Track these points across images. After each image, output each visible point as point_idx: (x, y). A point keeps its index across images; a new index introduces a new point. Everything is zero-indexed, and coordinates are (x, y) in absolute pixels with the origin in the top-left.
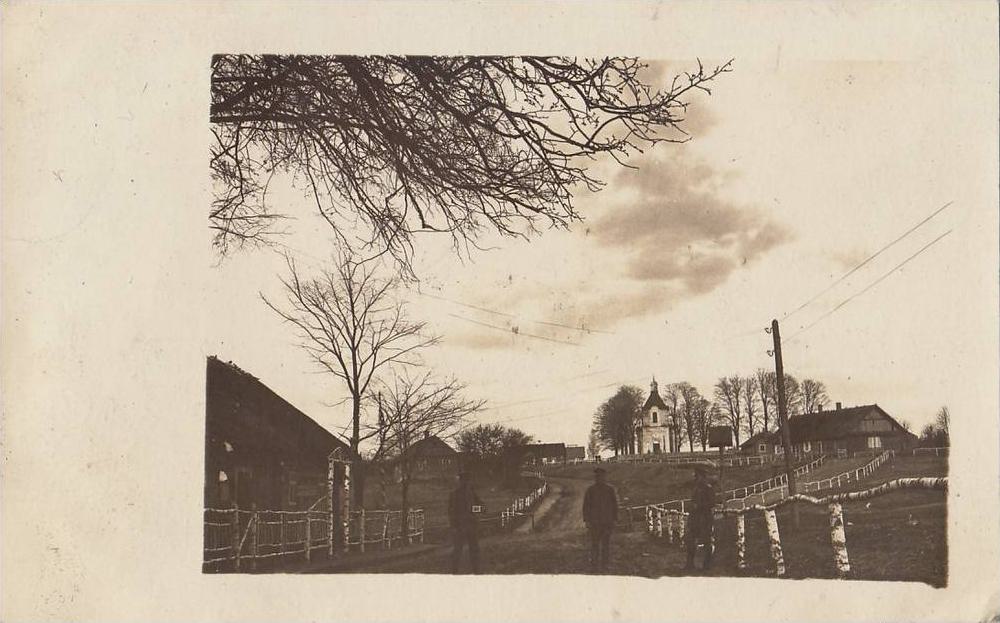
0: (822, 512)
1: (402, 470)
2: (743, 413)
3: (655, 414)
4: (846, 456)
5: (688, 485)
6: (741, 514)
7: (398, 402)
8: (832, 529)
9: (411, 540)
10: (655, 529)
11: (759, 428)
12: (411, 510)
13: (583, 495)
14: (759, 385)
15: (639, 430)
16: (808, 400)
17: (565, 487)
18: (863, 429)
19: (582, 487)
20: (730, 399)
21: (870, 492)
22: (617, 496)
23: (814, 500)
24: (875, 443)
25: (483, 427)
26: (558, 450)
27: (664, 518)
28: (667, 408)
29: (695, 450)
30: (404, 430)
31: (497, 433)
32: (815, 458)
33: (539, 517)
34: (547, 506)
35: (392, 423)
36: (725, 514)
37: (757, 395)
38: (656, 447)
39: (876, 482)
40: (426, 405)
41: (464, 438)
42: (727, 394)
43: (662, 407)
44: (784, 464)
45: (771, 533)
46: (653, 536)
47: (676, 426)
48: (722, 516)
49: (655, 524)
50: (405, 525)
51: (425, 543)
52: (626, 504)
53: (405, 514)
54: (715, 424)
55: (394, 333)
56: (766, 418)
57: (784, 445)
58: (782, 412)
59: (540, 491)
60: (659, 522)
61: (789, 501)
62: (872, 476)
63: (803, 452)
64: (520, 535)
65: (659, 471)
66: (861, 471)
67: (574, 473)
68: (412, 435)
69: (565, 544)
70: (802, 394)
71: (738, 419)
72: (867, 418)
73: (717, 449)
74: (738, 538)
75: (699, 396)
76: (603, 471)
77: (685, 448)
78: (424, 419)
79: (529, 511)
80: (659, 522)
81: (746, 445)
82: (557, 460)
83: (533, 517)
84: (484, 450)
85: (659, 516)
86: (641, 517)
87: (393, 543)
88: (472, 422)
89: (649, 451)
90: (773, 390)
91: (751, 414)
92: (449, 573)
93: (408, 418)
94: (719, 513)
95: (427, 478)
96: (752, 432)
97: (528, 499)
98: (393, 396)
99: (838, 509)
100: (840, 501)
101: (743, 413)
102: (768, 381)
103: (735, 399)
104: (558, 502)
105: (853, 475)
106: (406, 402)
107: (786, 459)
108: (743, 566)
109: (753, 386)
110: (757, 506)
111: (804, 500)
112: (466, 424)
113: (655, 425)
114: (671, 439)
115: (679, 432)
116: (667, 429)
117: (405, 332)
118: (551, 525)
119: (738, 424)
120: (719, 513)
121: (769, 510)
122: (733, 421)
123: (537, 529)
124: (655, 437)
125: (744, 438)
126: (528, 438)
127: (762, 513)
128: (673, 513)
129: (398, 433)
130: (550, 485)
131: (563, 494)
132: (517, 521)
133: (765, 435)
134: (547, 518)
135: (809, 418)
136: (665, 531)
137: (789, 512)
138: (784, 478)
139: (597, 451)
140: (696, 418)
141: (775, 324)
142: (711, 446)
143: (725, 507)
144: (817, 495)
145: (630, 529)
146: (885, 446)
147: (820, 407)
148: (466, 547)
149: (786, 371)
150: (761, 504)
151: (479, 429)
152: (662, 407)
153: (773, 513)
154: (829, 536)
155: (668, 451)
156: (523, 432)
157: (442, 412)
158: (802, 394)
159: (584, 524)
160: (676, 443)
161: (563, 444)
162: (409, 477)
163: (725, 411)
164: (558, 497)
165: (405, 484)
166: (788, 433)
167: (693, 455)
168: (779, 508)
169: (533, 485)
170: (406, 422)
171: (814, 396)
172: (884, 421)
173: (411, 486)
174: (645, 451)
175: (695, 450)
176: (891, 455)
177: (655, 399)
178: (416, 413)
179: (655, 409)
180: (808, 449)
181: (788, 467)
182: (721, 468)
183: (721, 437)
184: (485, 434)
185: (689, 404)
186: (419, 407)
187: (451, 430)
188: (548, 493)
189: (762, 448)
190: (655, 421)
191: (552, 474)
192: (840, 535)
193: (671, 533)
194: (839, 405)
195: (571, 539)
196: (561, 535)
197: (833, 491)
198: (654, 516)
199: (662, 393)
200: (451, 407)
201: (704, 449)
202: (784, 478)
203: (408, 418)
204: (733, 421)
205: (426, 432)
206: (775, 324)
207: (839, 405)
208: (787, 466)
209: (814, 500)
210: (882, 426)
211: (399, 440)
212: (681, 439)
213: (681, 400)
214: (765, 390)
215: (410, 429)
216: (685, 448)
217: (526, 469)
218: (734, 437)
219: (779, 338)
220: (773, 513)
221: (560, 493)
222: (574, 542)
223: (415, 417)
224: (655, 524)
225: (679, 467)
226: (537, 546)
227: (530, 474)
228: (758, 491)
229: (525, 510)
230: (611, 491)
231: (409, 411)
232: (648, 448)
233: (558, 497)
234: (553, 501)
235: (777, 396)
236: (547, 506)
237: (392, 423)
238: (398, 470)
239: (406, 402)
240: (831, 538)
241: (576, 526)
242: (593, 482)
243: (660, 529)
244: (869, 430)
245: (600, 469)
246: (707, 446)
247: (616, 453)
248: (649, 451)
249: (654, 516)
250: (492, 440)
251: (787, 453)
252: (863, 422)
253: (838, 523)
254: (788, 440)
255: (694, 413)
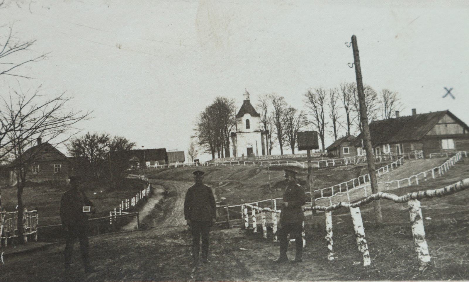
0: (403, 208)
1: (17, 174)
2: (328, 120)
3: (248, 121)
4: (422, 156)
5: (280, 184)
6: (328, 210)
7: (12, 112)
8: (412, 223)
9: (26, 238)
10: (251, 225)
11: (342, 133)
12: (26, 211)
13: (184, 194)
14: (341, 94)
15: (234, 135)
16: (386, 106)
17: (167, 188)
18: (438, 133)
19: (184, 187)
20: (315, 107)
21: (446, 190)
22: (215, 196)
23: (395, 197)
24: (448, 144)
25: (92, 134)
26: (160, 154)
27: (258, 215)
28: (258, 115)
29: (285, 153)
30: (18, 138)
31: (103, 140)
32: (394, 158)
33: (144, 216)
34: (150, 206)
35: (7, 131)
36: (314, 211)
37: (340, 103)
38: (250, 150)
39: (452, 180)
40: (38, 114)
41: (75, 145)
42: (312, 102)
43: (255, 114)
44: (366, 164)
45: (356, 228)
46: (249, 232)
47: (267, 132)
48: (310, 213)
49: (251, 220)
50: (20, 223)
51: (39, 240)
52: (223, 203)
53: (20, 214)
54: (303, 129)
55: (7, 48)
56: (349, 124)
57: (366, 148)
58: (363, 118)
59: (144, 192)
60: (254, 219)
61: (372, 199)
62: (446, 175)
63: (382, 153)
64: (131, 232)
65: (253, 173)
66: (436, 170)
67: (178, 175)
68: (26, 142)
69: (169, 241)
70: (380, 102)
71: (323, 125)
72: (440, 122)
73: (305, 152)
74: (326, 233)
75: (286, 104)
76: (201, 173)
77: (276, 151)
78: (36, 128)
79: (136, 210)
80: (254, 219)
81: (331, 149)
82: (160, 164)
83: (138, 215)
84: (92, 155)
85: (254, 213)
86: (236, 214)
87: (9, 241)
88: (79, 131)
89: (243, 155)
90: (354, 97)
91: (334, 121)
92: (152, 150)
93: (22, 126)
94: (308, 210)
95: (40, 181)
96: (336, 136)
97: (133, 200)
98: (7, 107)
99: (416, 205)
100: (419, 198)
101: (328, 120)
102: (350, 90)
103: (320, 107)
104: (161, 202)
105: (429, 175)
106: (20, 112)
107: (368, 160)
108: (332, 258)
109: (336, 95)
110: (343, 204)
111: (385, 198)
112: (75, 131)
113: (248, 130)
114: (263, 144)
115: (270, 137)
116: (259, 134)
117: (17, 48)
118: (155, 224)
119: (323, 128)
120: (308, 210)
121: (354, 207)
122: (319, 127)
123: (143, 227)
124: (247, 140)
125: (329, 141)
126: (132, 144)
127: (347, 210)
128: (266, 211)
129: (13, 140)
130: (153, 186)
131: (165, 195)
132: (124, 221)
133: (348, 140)
134: (151, 216)
135: (389, 122)
136: (260, 227)
137: (373, 208)
138: (366, 177)
139: (196, 155)
140: (285, 124)
141: (354, 40)
142: (300, 149)
143: (314, 205)
144: (399, 192)
145: (227, 226)
146: (459, 147)
147: (397, 112)
148: (77, 245)
149: (365, 82)
150: (346, 201)
151: (88, 137)
152: (255, 114)
153: (358, 209)
154: (409, 229)
155: (260, 154)
156: (127, 139)
157: (50, 121)
158: (380, 102)
159: (185, 222)
160: (267, 148)
161: (165, 149)
162: (23, 180)
163: (311, 118)
164: (161, 197)
165: (20, 187)
166: (369, 137)
167: (284, 158)
168: (364, 204)
169: (139, 186)
170: (20, 130)
171: (392, 103)
172: (456, 125)
173: (25, 189)
174: (239, 155)
175: (285, 153)
176: (463, 155)
177: (247, 108)
178: (30, 121)
179: (247, 116)
180: (387, 150)
181: (370, 169)
182: (310, 169)
183: (308, 141)
184: (93, 141)
185: (278, 113)
186: (32, 116)
187: (62, 137)
188: (152, 194)
189: (346, 151)
190: (248, 127)
191: (157, 177)
192: (419, 229)
193: (265, 228)
194: (414, 110)
195: (173, 236)
196: (164, 232)
197: (412, 189)
198: (250, 214)
199: (254, 103)
200: (62, 116)
201: (293, 153)
202: (366, 177)
203: (22, 126)
204: (319, 127)
205: (39, 139)
206: (354, 40)
207: (414, 110)
208: (369, 166)
209: (395, 197)
210: (453, 129)
211: (14, 147)
212: (272, 143)
213: (271, 109)
214: (346, 97)
215: (24, 136)
216: (276, 151)
217: (130, 172)
218: (320, 141)
219: (358, 51)
220: (358, 209)
221: (163, 194)
222: (176, 238)
223: (28, 125)
224: (251, 220)
225: (271, 168)
226: (142, 242)
227: (135, 176)
228: (344, 190)
229: (131, 209)
230: (209, 190)
231: (22, 120)
232: (242, 151)
233: (161, 197)
234: (157, 201)
235: (358, 104)
236: (150, 206)
237: (7, 131)
238: (13, 174)
239: (20, 112)
240: (411, 232)
241: (178, 223)
242: (194, 183)
243: (255, 225)
244: (443, 133)
245: (199, 173)
246: (296, 150)
247: (213, 157)
248: (243, 155)
249: (250, 214)
250: (100, 145)
251: (368, 155)
252: (437, 126)
253: (418, 217)
254: (370, 143)
255: (284, 120)
